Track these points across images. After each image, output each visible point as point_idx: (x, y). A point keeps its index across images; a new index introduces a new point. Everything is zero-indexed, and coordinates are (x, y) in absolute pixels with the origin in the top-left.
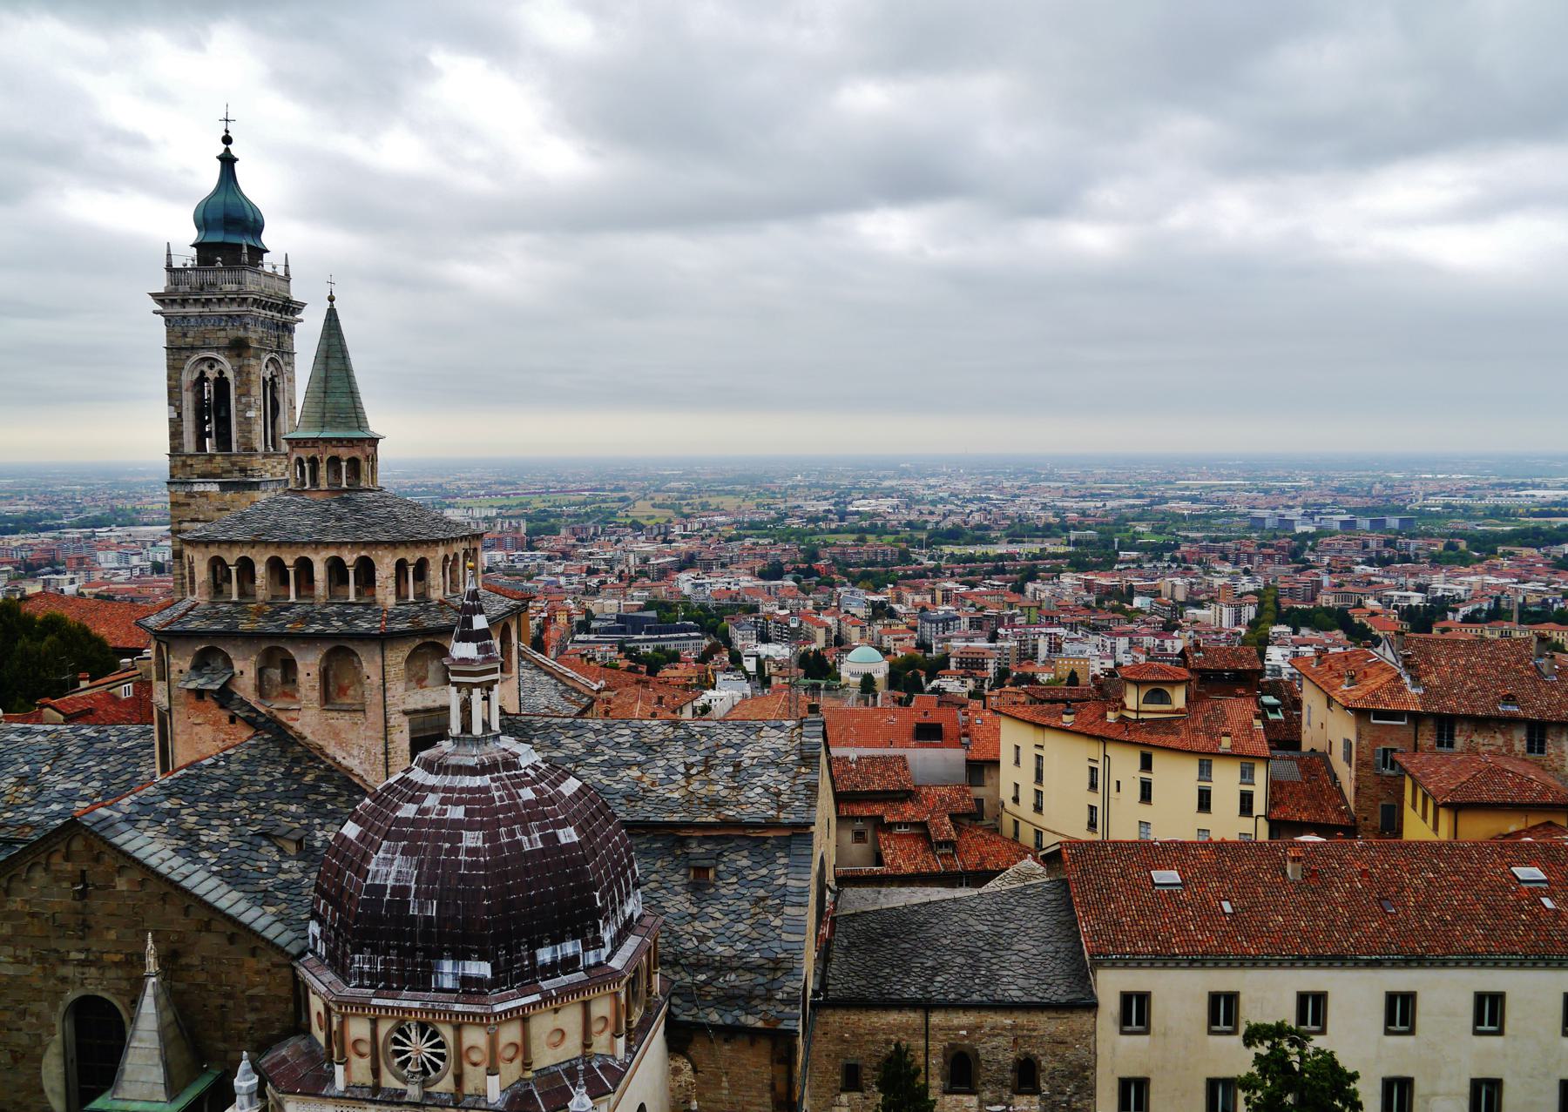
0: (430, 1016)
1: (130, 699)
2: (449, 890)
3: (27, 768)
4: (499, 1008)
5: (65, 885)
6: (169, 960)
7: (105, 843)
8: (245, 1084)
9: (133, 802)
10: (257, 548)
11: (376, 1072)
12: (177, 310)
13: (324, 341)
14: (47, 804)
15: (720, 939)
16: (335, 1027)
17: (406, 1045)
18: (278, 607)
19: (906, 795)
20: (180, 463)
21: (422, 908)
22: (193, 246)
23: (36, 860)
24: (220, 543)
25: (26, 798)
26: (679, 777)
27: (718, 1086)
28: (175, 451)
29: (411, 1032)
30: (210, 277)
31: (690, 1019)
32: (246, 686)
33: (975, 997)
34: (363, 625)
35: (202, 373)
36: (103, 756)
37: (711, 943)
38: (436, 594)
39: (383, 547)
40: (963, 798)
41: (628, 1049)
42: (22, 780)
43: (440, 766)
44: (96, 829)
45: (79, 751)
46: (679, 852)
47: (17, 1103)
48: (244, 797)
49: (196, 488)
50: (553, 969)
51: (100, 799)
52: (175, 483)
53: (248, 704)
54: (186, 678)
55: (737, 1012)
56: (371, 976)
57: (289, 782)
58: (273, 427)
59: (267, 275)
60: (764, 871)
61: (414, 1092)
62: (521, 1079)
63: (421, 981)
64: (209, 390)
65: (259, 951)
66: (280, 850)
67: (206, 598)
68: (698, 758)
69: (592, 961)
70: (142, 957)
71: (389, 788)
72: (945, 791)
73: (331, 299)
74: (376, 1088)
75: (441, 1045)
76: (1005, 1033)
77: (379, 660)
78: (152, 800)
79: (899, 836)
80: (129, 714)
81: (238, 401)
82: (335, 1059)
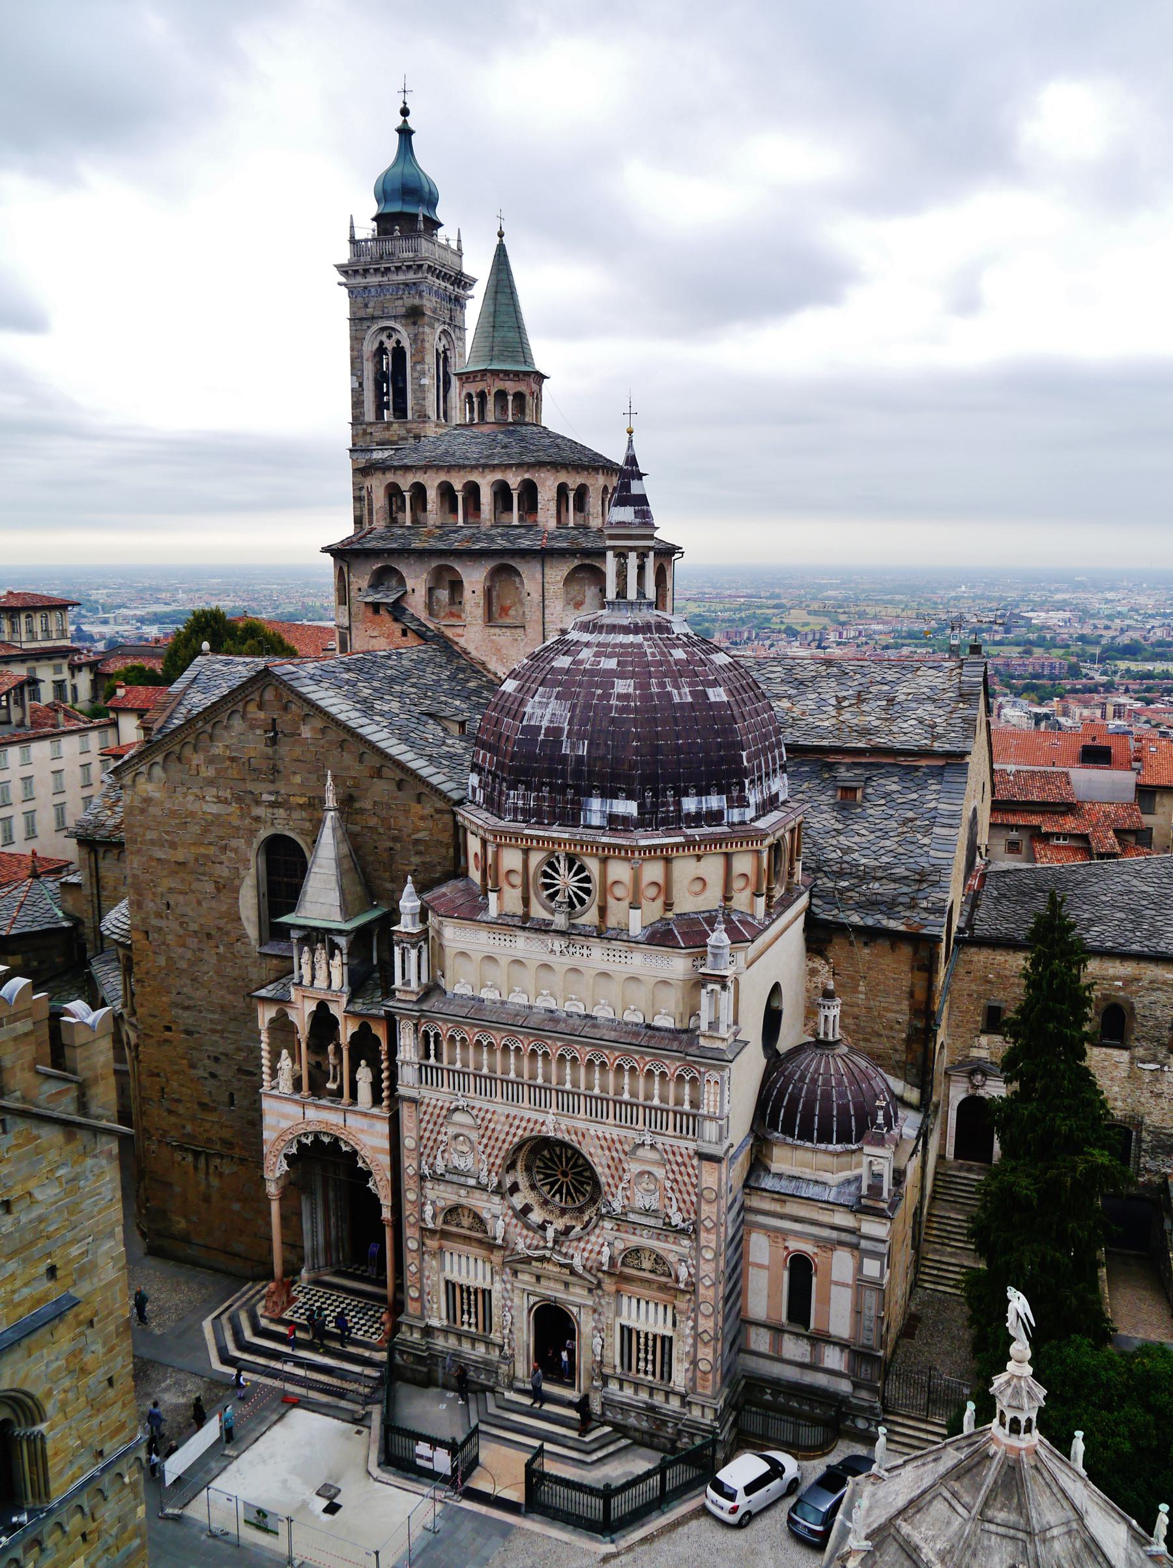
0: (578, 848)
2: (600, 731)
4: (643, 843)
5: (259, 732)
6: (347, 803)
7: (292, 692)
8: (409, 905)
10: (428, 474)
11: (526, 901)
12: (359, 280)
13: (494, 277)
15: (865, 852)
16: (490, 861)
17: (554, 878)
18: (445, 531)
19: (1069, 808)
21: (574, 747)
22: (373, 219)
23: (234, 708)
24: (396, 468)
26: (831, 708)
27: (855, 990)
28: (357, 421)
29: (559, 862)
30: (388, 246)
31: (831, 918)
32: (416, 604)
33: (1135, 947)
34: (525, 543)
35: (382, 343)
37: (856, 855)
38: (595, 523)
39: (544, 469)
40: (1130, 815)
41: (768, 914)
43: (595, 625)
46: (826, 776)
47: (219, 928)
48: (413, 685)
50: (697, 819)
52: (356, 451)
53: (418, 620)
55: (879, 917)
56: (524, 811)
57: (454, 684)
58: (445, 397)
59: (440, 246)
60: (915, 796)
61: (560, 921)
62: (662, 919)
63: (571, 818)
64: (387, 361)
65: (423, 798)
66: (445, 730)
67: (383, 523)
68: (851, 692)
69: (736, 819)
70: (323, 801)
71: (546, 649)
72: (1108, 808)
73: (501, 235)
74: (526, 917)
75: (587, 879)
76: (1165, 988)
77: (539, 576)
79: (1057, 847)
81: (413, 368)
82: (489, 887)
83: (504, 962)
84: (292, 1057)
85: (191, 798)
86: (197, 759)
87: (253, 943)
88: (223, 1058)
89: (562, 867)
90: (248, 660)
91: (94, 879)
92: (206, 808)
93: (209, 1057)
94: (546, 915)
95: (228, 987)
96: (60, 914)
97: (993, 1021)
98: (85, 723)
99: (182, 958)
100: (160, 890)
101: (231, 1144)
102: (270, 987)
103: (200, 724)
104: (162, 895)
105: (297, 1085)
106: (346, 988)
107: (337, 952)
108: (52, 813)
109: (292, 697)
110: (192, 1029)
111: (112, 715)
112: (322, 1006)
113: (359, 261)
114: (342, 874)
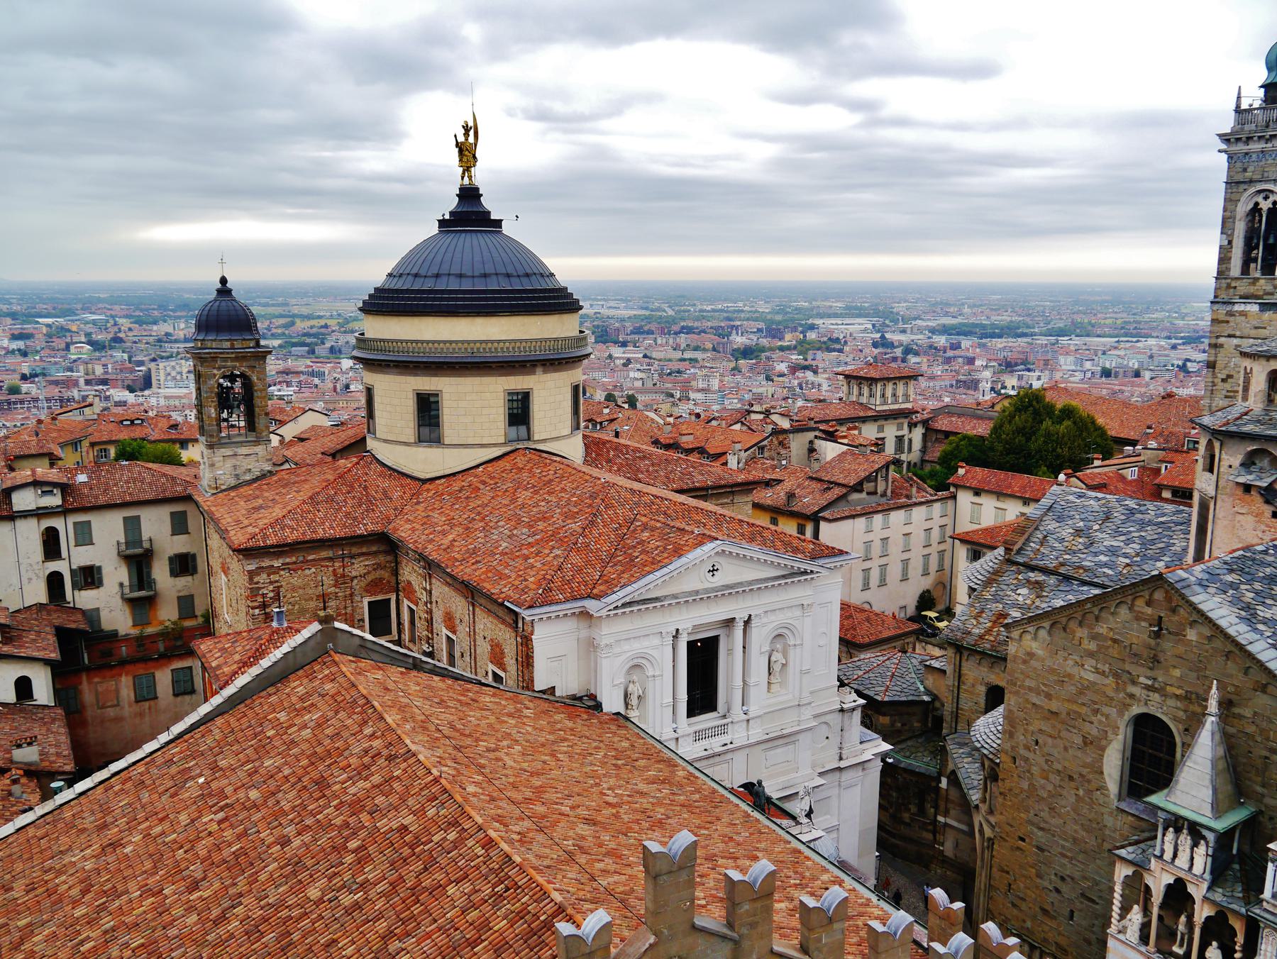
1: (1134, 480)
3: (1081, 524)
5: (1143, 624)
6: (1226, 705)
9: (1203, 571)
12: (1241, 147)
14: (1096, 554)
20: (1225, 285)
25: (1080, 547)
28: (1221, 274)
35: (1257, 204)
36: (1143, 525)
42: (1078, 532)
44: (1178, 586)
45: (1123, 517)
49: (1236, 308)
51: (1138, 559)
52: (1218, 302)
54: (1236, 473)
78: (1218, 571)
80: (1134, 492)
85: (1070, 662)
86: (1081, 633)
87: (1112, 796)
88: (1069, 879)
90: (1100, 495)
91: (957, 675)
92: (1082, 673)
93: (1056, 874)
95: (1082, 825)
96: (922, 689)
98: (931, 495)
99: (1043, 788)
100: (1031, 728)
101: (1065, 951)
102: (1130, 849)
103: (1089, 605)
104: (1033, 733)
105: (1144, 939)
106: (1207, 876)
107: (1202, 842)
108: (900, 565)
109: (1181, 603)
110: (1044, 847)
111: (952, 489)
113: (1242, 129)
114: (1216, 773)
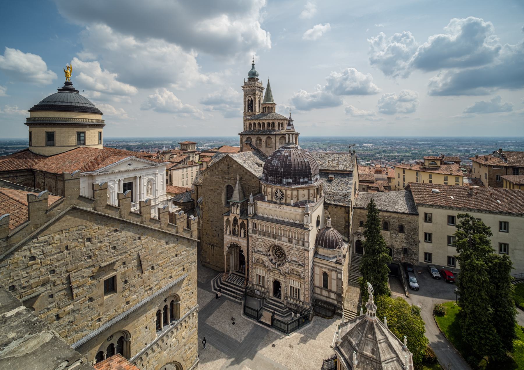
56: (272, 181)
61: (278, 201)
74: (272, 201)
75: (283, 194)
83: (268, 210)
84: (230, 227)
89: (279, 191)
94: (276, 201)
97: (361, 224)
105: (230, 233)
112: (235, 217)
